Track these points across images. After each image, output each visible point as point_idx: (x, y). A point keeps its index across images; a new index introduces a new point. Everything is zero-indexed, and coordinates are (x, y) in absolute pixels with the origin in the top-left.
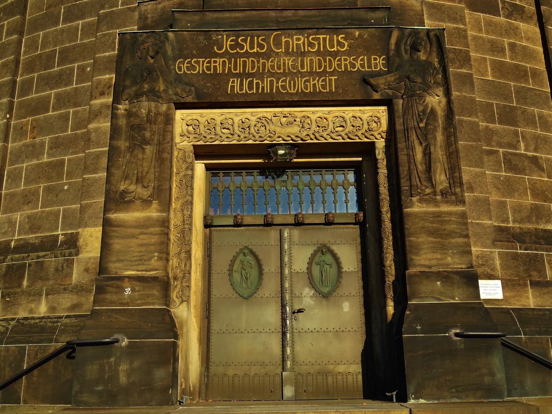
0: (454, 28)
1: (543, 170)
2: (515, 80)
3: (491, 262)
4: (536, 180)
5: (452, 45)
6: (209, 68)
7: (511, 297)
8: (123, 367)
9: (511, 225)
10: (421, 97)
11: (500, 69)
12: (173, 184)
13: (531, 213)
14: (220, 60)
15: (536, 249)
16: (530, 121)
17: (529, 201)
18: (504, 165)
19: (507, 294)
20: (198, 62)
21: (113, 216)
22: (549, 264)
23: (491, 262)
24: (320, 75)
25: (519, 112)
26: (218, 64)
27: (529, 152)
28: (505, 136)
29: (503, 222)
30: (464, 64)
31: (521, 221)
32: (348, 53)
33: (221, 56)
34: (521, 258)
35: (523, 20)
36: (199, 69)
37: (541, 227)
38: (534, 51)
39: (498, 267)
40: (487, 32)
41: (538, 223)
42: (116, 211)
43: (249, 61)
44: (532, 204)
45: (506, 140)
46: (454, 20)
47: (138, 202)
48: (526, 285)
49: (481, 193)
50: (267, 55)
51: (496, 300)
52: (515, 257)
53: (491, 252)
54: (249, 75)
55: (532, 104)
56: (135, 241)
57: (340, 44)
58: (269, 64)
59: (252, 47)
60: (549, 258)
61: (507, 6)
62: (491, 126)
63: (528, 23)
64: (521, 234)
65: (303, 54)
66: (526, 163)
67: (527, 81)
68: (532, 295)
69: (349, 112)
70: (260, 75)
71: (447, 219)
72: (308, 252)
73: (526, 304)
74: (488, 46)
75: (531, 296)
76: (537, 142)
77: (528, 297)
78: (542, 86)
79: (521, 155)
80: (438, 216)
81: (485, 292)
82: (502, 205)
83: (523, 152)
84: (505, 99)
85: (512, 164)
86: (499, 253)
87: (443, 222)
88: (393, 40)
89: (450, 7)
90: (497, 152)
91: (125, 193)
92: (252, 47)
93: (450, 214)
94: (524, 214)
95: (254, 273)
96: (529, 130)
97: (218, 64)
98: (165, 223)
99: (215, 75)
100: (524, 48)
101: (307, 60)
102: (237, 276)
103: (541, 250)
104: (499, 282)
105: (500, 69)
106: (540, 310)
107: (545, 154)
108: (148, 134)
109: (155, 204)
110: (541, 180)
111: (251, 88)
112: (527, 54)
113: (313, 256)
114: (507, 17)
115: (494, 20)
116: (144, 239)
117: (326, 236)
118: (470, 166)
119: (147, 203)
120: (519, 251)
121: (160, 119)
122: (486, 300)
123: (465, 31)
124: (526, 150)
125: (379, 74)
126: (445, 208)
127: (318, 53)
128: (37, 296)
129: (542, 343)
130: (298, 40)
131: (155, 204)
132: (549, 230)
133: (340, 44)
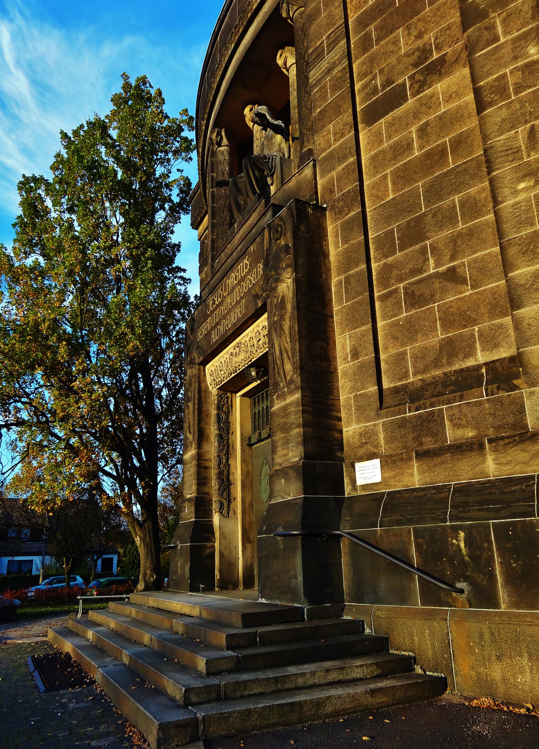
0: (343, 169)
1: (464, 281)
3: (375, 437)
4: (451, 301)
5: (341, 192)
7: (390, 478)
9: (411, 380)
10: (275, 289)
12: (208, 424)
13: (441, 352)
15: (432, 405)
17: (440, 335)
18: (405, 303)
19: (387, 475)
22: (451, 421)
23: (375, 437)
25: (429, 217)
27: (442, 265)
28: (407, 264)
29: (400, 379)
30: (352, 205)
34: (410, 423)
37: (457, 367)
39: (382, 442)
41: (450, 363)
44: (443, 340)
48: (410, 459)
49: (366, 356)
51: (373, 484)
52: (402, 424)
53: (375, 425)
55: (449, 194)
60: (451, 413)
62: (390, 259)
64: (422, 388)
68: (418, 470)
71: (289, 411)
73: (409, 484)
75: (416, 472)
76: (455, 245)
77: (412, 475)
80: (286, 410)
81: (363, 476)
82: (401, 357)
83: (432, 271)
84: (410, 212)
87: (288, 415)
90: (396, 290)
103: (439, 404)
106: (424, 489)
107: (469, 255)
110: (459, 299)
115: (398, 113)
118: (356, 328)
120: (408, 414)
122: (365, 487)
124: (437, 265)
129: (401, 536)
132: (468, 368)
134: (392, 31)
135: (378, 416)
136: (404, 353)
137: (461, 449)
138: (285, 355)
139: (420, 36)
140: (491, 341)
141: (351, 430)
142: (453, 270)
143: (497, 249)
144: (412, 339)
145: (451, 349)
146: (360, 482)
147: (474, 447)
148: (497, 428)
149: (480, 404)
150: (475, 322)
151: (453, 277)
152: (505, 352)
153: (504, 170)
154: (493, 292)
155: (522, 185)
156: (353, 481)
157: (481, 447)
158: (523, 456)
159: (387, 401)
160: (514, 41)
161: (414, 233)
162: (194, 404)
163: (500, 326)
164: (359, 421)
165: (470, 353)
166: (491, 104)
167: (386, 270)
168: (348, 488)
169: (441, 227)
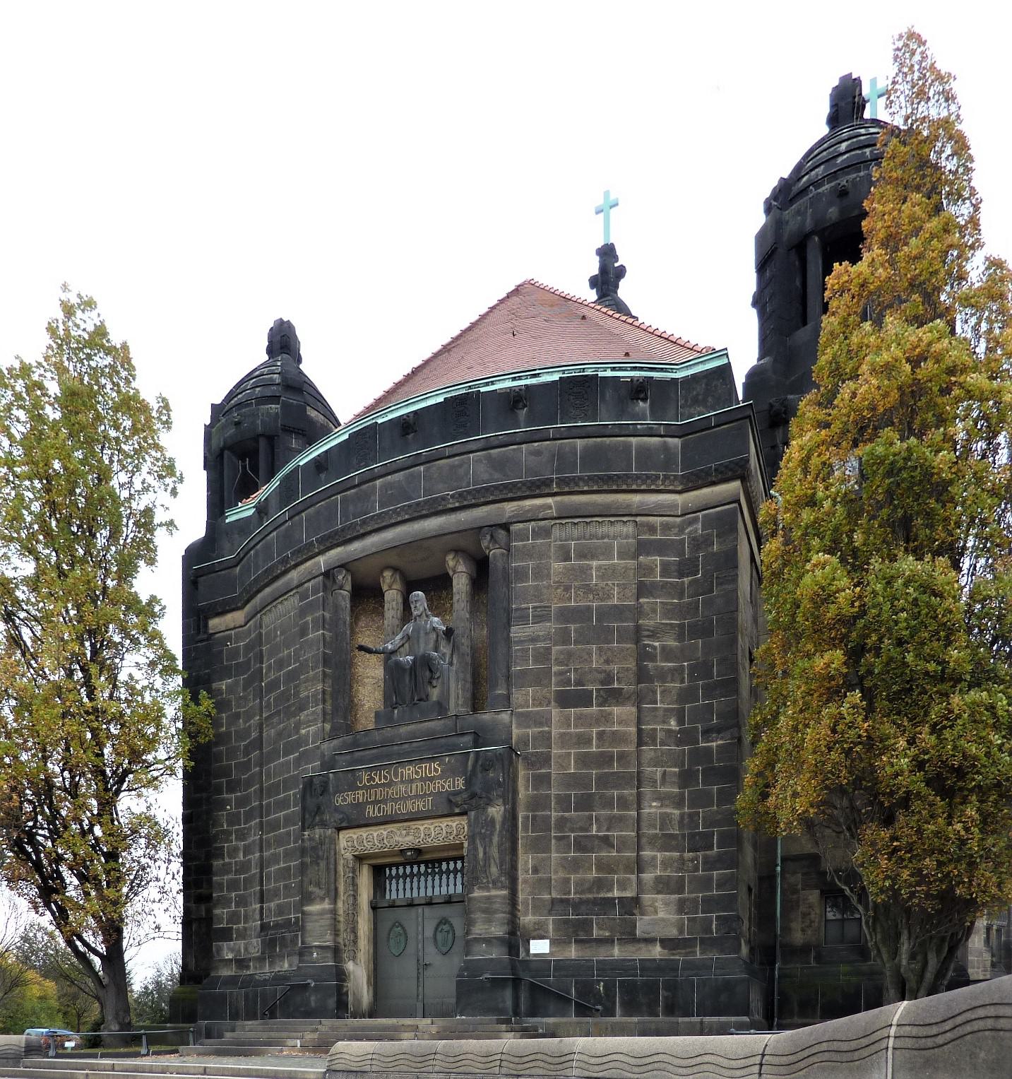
6: (354, 799)
8: (313, 998)
11: (584, 760)
16: (608, 804)
17: (594, 874)
20: (348, 795)
21: (306, 908)
24: (422, 797)
26: (360, 796)
29: (565, 894)
31: (582, 892)
32: (440, 777)
35: (618, 704)
36: (349, 800)
37: (602, 895)
38: (625, 733)
40: (576, 726)
41: (598, 893)
42: (308, 905)
43: (378, 791)
45: (580, 824)
46: (541, 724)
48: (571, 943)
50: (389, 785)
52: (566, 922)
54: (380, 802)
55: (613, 788)
57: (436, 770)
58: (390, 792)
59: (380, 780)
61: (602, 692)
62: (566, 814)
63: (623, 704)
65: (412, 781)
66: (596, 843)
67: (611, 766)
69: (444, 823)
70: (384, 801)
74: (574, 740)
79: (593, 836)
82: (567, 881)
85: (581, 846)
88: (470, 763)
89: (538, 712)
90: (569, 836)
91: (311, 893)
92: (380, 780)
94: (587, 885)
96: (605, 812)
97: (360, 796)
98: (334, 912)
100: (614, 733)
104: (547, 942)
105: (584, 760)
108: (321, 853)
111: (379, 812)
112: (617, 738)
114: (599, 705)
116: (323, 922)
117: (446, 911)
119: (323, 899)
121: (327, 840)
123: (550, 733)
124: (597, 831)
127: (421, 779)
128: (282, 957)
130: (409, 771)
131: (327, 900)
133: (436, 770)
134: (588, 643)
135: (550, 914)
136: (570, 879)
137: (601, 941)
139: (607, 662)
141: (527, 919)
142: (607, 837)
143: (634, 834)
144: (576, 871)
145: (600, 884)
146: (532, 951)
147: (609, 941)
148: (622, 934)
149: (614, 919)
150: (616, 873)
151: (606, 841)
152: (628, 894)
153: (646, 790)
154: (628, 858)
155: (654, 804)
156: (528, 950)
157: (613, 941)
160: (666, 710)
161: (585, 803)
163: (629, 879)
164: (534, 914)
165: (611, 890)
166: (646, 744)
167: (562, 823)
168: (522, 955)
169: (604, 808)
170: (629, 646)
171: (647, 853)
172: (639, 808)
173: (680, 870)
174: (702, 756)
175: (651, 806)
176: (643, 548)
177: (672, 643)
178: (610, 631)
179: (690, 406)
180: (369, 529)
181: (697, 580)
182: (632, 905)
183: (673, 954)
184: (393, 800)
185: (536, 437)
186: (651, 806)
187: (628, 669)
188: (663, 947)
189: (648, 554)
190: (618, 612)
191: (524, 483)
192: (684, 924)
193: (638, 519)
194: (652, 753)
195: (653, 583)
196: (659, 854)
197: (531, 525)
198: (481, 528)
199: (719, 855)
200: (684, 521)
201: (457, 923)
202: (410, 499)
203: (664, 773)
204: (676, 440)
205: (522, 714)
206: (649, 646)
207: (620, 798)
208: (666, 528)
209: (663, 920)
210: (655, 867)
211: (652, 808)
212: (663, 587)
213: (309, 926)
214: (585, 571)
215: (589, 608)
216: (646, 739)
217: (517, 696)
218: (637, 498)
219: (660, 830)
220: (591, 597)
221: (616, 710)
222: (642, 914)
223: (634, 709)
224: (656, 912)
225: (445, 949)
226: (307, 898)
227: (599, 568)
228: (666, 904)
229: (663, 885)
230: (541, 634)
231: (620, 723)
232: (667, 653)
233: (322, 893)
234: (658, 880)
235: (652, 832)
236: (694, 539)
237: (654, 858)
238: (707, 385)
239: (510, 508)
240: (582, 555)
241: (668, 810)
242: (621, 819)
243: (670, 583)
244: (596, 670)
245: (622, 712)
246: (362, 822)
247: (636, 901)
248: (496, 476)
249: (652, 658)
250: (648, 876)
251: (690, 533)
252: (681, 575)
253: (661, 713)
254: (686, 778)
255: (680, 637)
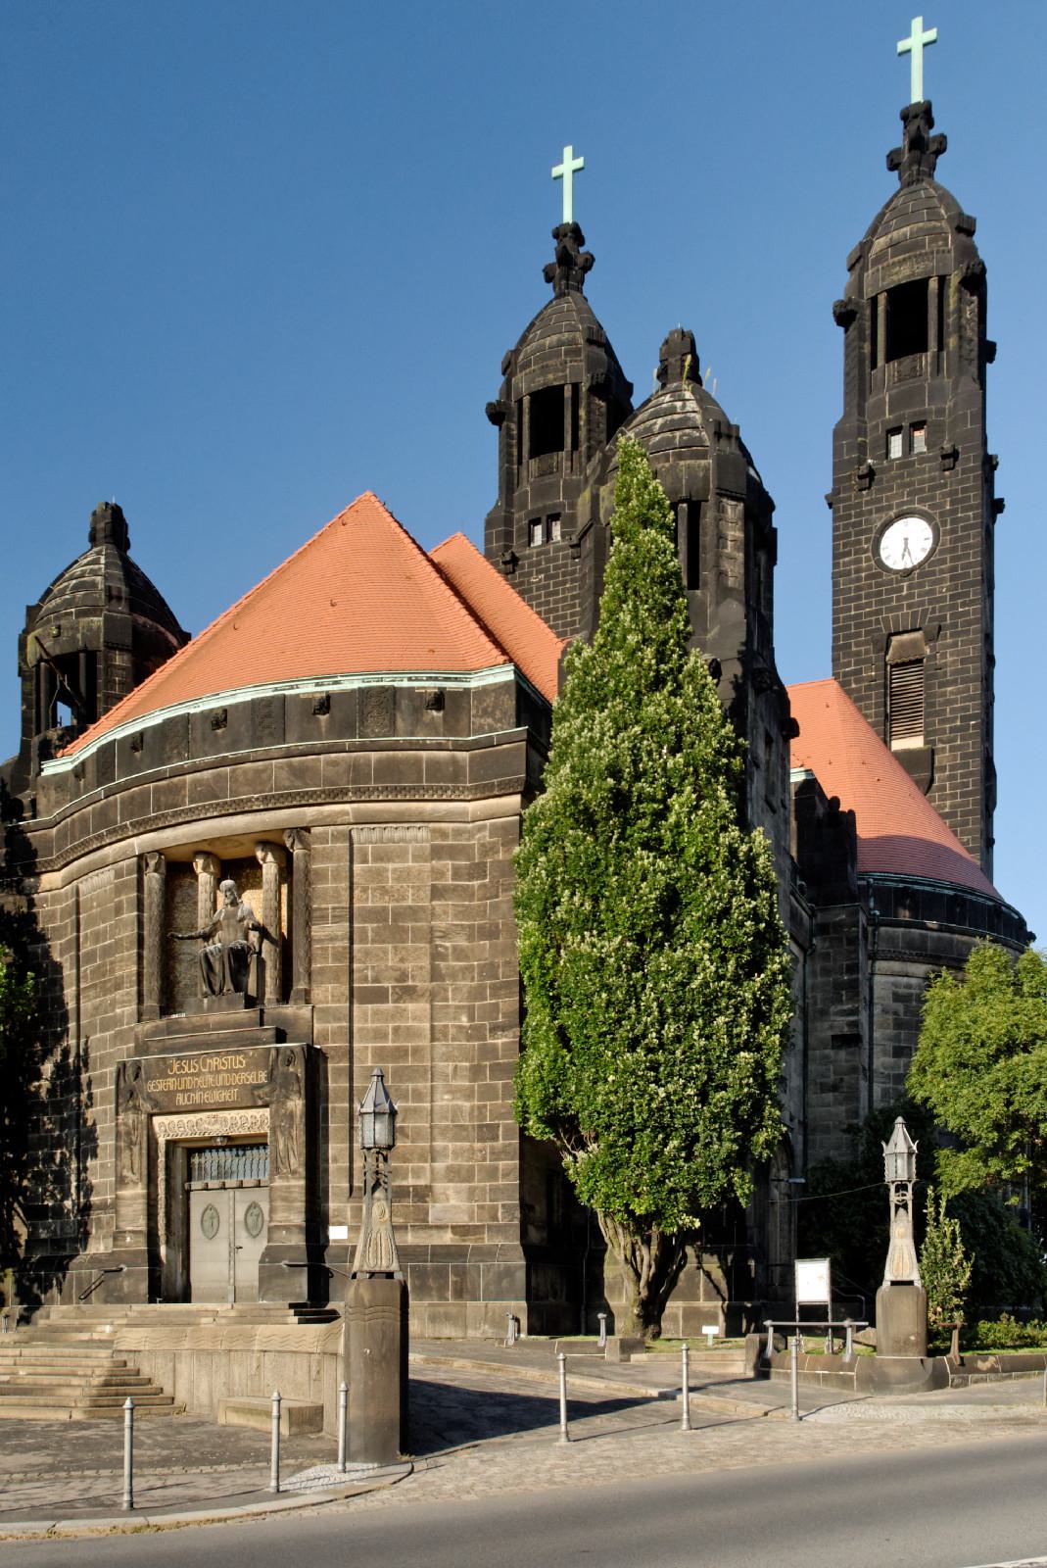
1: (407, 1137)
2: (393, 1062)
8: (126, 1283)
10: (284, 1103)
11: (380, 1054)
14: (172, 1080)
21: (119, 1193)
32: (245, 1070)
33: (172, 1076)
35: (412, 1000)
38: (419, 1028)
40: (373, 1022)
47: (131, 1184)
50: (197, 1075)
55: (407, 1081)
56: (131, 1209)
61: (397, 990)
72: (245, 1207)
74: (371, 1035)
78: (423, 1061)
86: (352, 1207)
87: (291, 1192)
89: (336, 1008)
93: (295, 1186)
95: (215, 1222)
99: (169, 1091)
100: (408, 1028)
101: (221, 1077)
102: (207, 1224)
108: (134, 1139)
109: (140, 1185)
112: (411, 1033)
113: (248, 1209)
114: (395, 1001)
119: (136, 1183)
125: (260, 1086)
126: (293, 1182)
127: (227, 1071)
130: (214, 1062)
131: (140, 1185)
134: (384, 942)
135: (348, 1202)
138: (291, 1153)
139: (402, 960)
140: (417, 1173)
150: (409, 1161)
152: (422, 1182)
153: (438, 1083)
154: (423, 1148)
155: (446, 1097)
156: (327, 1237)
157: (406, 1227)
158: (424, 1235)
159: (354, 1194)
160: (459, 1007)
162: (141, 1148)
163: (423, 1168)
165: (405, 1178)
166: (438, 1040)
170: (422, 945)
171: (439, 1144)
172: (432, 1101)
173: (470, 1159)
174: (488, 1052)
175: (443, 1099)
176: (437, 852)
177: (463, 943)
178: (405, 930)
179: (481, 717)
180: (180, 820)
181: (484, 885)
182: (423, 1194)
183: (464, 1241)
184: (201, 1090)
185: (335, 749)
186: (443, 1099)
187: (421, 968)
188: (454, 1233)
189: (440, 859)
190: (414, 913)
191: (324, 792)
192: (473, 1212)
193: (431, 825)
194: (444, 1049)
195: (444, 886)
196: (450, 1145)
197: (330, 829)
198: (284, 830)
199: (505, 1146)
200: (473, 828)
201: (265, 1207)
202: (218, 798)
203: (456, 1066)
204: (464, 753)
205: (322, 1010)
206: (441, 946)
207: (414, 1091)
208: (458, 833)
209: (455, 1207)
210: (446, 1156)
211: (444, 1101)
212: (454, 890)
213: (123, 1211)
214: (379, 874)
215: (385, 909)
216: (437, 1035)
217: (318, 993)
218: (430, 805)
219: (452, 1121)
220: (387, 898)
221: (410, 1006)
222: (434, 1202)
223: (428, 1006)
224: (448, 1199)
225: (255, 1233)
226: (121, 1181)
227: (395, 870)
228: (457, 1192)
229: (454, 1174)
230: (340, 933)
231: (414, 1019)
232: (459, 954)
233: (135, 1178)
234: (450, 1169)
235: (444, 1123)
236: (483, 845)
237: (445, 1148)
238: (496, 698)
239: (311, 812)
240: (378, 858)
241: (459, 1103)
242: (415, 1110)
243: (462, 886)
244: (392, 968)
245: (417, 1008)
246: (174, 1110)
247: (429, 1188)
248: (297, 783)
249: (444, 957)
250: (440, 1165)
251: (479, 839)
252: (471, 877)
253: (451, 1010)
254: (476, 1072)
255: (470, 938)
